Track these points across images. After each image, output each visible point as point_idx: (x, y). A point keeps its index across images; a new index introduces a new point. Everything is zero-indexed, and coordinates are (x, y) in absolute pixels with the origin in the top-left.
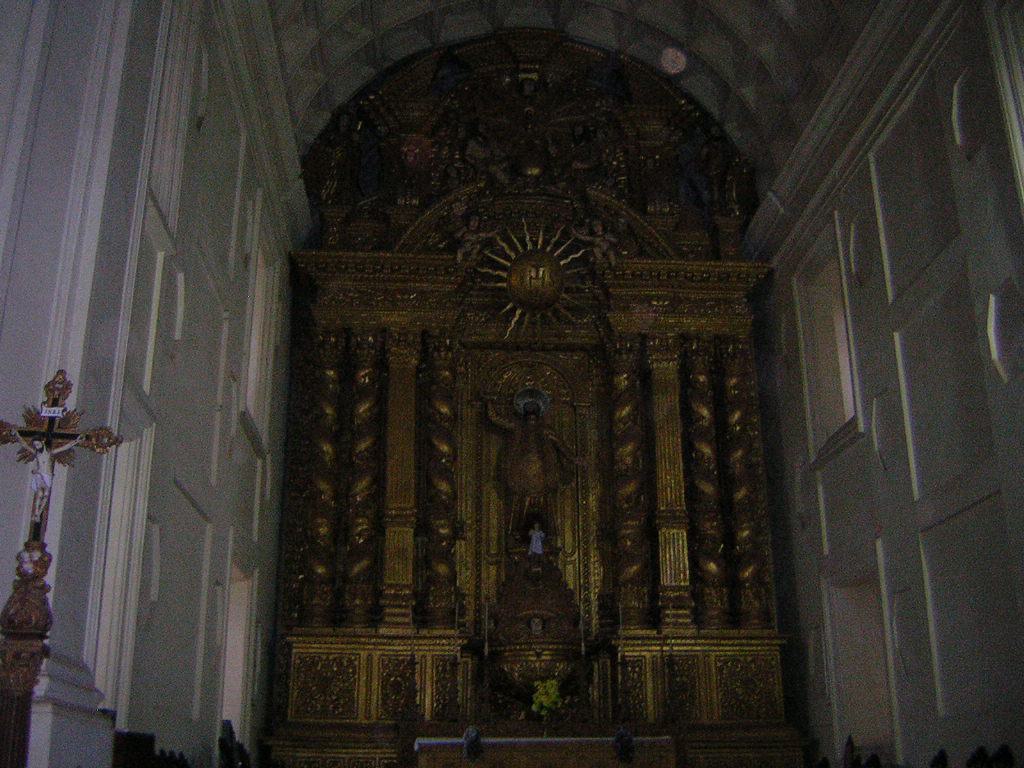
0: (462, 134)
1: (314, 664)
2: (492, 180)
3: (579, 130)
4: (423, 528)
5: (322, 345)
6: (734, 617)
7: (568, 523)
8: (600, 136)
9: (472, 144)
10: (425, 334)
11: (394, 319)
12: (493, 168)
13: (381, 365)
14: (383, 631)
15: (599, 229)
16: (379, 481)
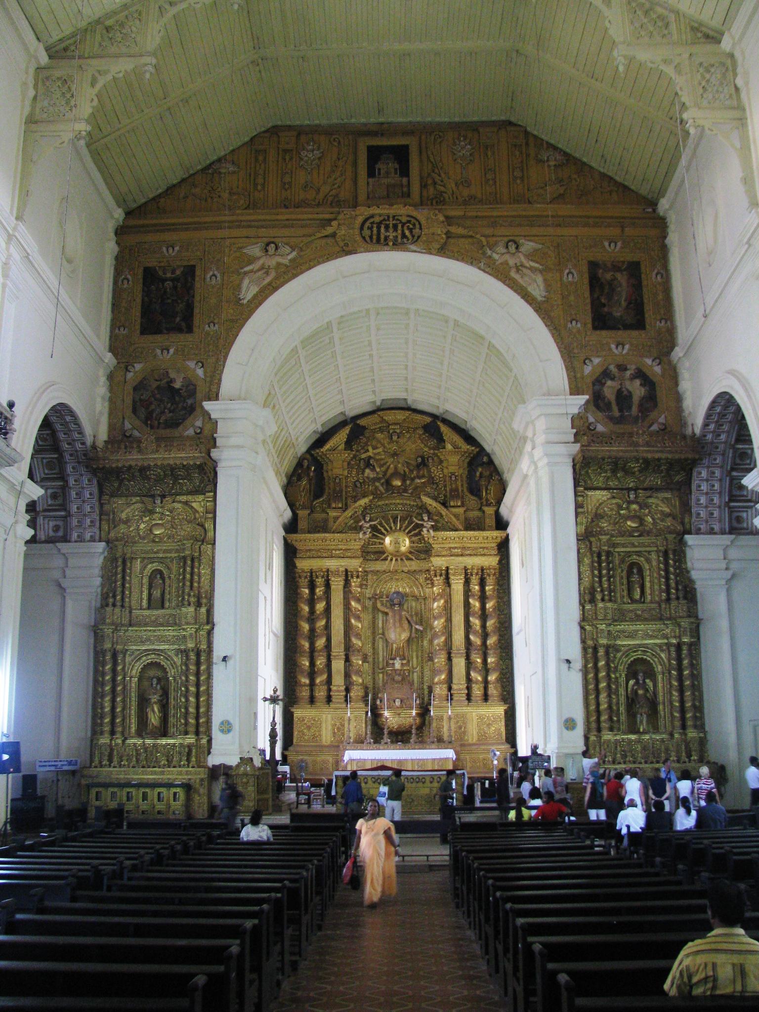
0: (362, 464)
1: (303, 720)
2: (376, 488)
3: (420, 460)
4: (347, 660)
5: (300, 577)
6: (486, 697)
7: (415, 654)
8: (430, 461)
9: (367, 471)
10: (346, 571)
11: (332, 564)
12: (377, 484)
13: (328, 585)
14: (332, 705)
15: (426, 518)
16: (329, 640)
